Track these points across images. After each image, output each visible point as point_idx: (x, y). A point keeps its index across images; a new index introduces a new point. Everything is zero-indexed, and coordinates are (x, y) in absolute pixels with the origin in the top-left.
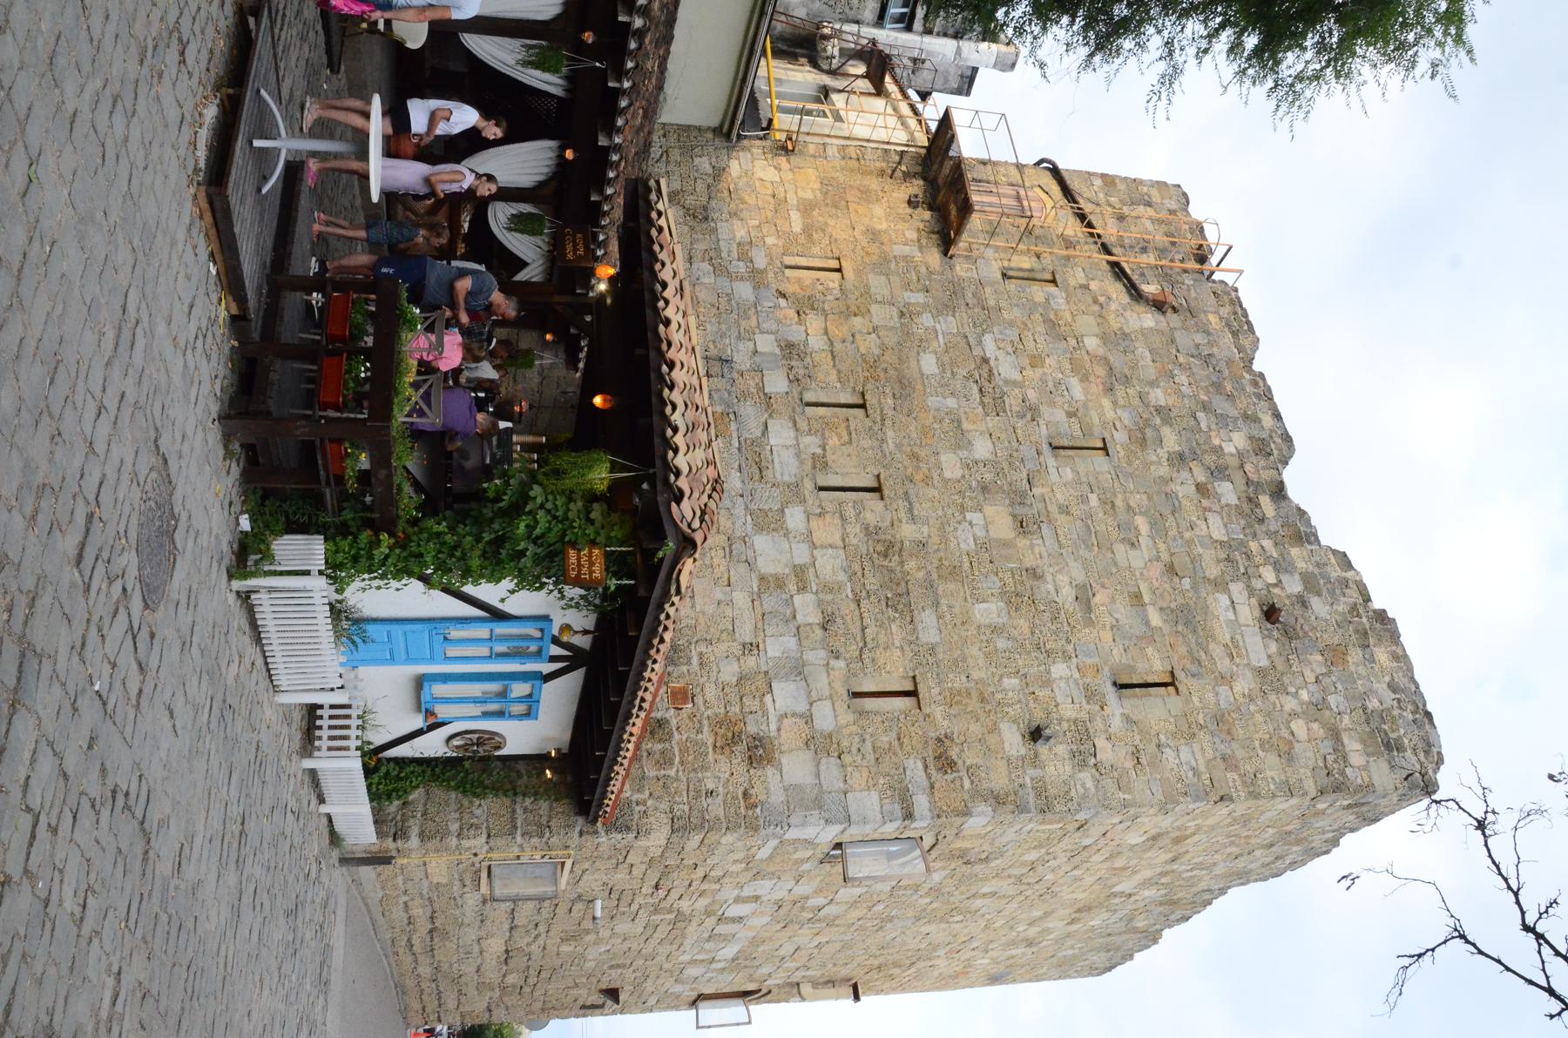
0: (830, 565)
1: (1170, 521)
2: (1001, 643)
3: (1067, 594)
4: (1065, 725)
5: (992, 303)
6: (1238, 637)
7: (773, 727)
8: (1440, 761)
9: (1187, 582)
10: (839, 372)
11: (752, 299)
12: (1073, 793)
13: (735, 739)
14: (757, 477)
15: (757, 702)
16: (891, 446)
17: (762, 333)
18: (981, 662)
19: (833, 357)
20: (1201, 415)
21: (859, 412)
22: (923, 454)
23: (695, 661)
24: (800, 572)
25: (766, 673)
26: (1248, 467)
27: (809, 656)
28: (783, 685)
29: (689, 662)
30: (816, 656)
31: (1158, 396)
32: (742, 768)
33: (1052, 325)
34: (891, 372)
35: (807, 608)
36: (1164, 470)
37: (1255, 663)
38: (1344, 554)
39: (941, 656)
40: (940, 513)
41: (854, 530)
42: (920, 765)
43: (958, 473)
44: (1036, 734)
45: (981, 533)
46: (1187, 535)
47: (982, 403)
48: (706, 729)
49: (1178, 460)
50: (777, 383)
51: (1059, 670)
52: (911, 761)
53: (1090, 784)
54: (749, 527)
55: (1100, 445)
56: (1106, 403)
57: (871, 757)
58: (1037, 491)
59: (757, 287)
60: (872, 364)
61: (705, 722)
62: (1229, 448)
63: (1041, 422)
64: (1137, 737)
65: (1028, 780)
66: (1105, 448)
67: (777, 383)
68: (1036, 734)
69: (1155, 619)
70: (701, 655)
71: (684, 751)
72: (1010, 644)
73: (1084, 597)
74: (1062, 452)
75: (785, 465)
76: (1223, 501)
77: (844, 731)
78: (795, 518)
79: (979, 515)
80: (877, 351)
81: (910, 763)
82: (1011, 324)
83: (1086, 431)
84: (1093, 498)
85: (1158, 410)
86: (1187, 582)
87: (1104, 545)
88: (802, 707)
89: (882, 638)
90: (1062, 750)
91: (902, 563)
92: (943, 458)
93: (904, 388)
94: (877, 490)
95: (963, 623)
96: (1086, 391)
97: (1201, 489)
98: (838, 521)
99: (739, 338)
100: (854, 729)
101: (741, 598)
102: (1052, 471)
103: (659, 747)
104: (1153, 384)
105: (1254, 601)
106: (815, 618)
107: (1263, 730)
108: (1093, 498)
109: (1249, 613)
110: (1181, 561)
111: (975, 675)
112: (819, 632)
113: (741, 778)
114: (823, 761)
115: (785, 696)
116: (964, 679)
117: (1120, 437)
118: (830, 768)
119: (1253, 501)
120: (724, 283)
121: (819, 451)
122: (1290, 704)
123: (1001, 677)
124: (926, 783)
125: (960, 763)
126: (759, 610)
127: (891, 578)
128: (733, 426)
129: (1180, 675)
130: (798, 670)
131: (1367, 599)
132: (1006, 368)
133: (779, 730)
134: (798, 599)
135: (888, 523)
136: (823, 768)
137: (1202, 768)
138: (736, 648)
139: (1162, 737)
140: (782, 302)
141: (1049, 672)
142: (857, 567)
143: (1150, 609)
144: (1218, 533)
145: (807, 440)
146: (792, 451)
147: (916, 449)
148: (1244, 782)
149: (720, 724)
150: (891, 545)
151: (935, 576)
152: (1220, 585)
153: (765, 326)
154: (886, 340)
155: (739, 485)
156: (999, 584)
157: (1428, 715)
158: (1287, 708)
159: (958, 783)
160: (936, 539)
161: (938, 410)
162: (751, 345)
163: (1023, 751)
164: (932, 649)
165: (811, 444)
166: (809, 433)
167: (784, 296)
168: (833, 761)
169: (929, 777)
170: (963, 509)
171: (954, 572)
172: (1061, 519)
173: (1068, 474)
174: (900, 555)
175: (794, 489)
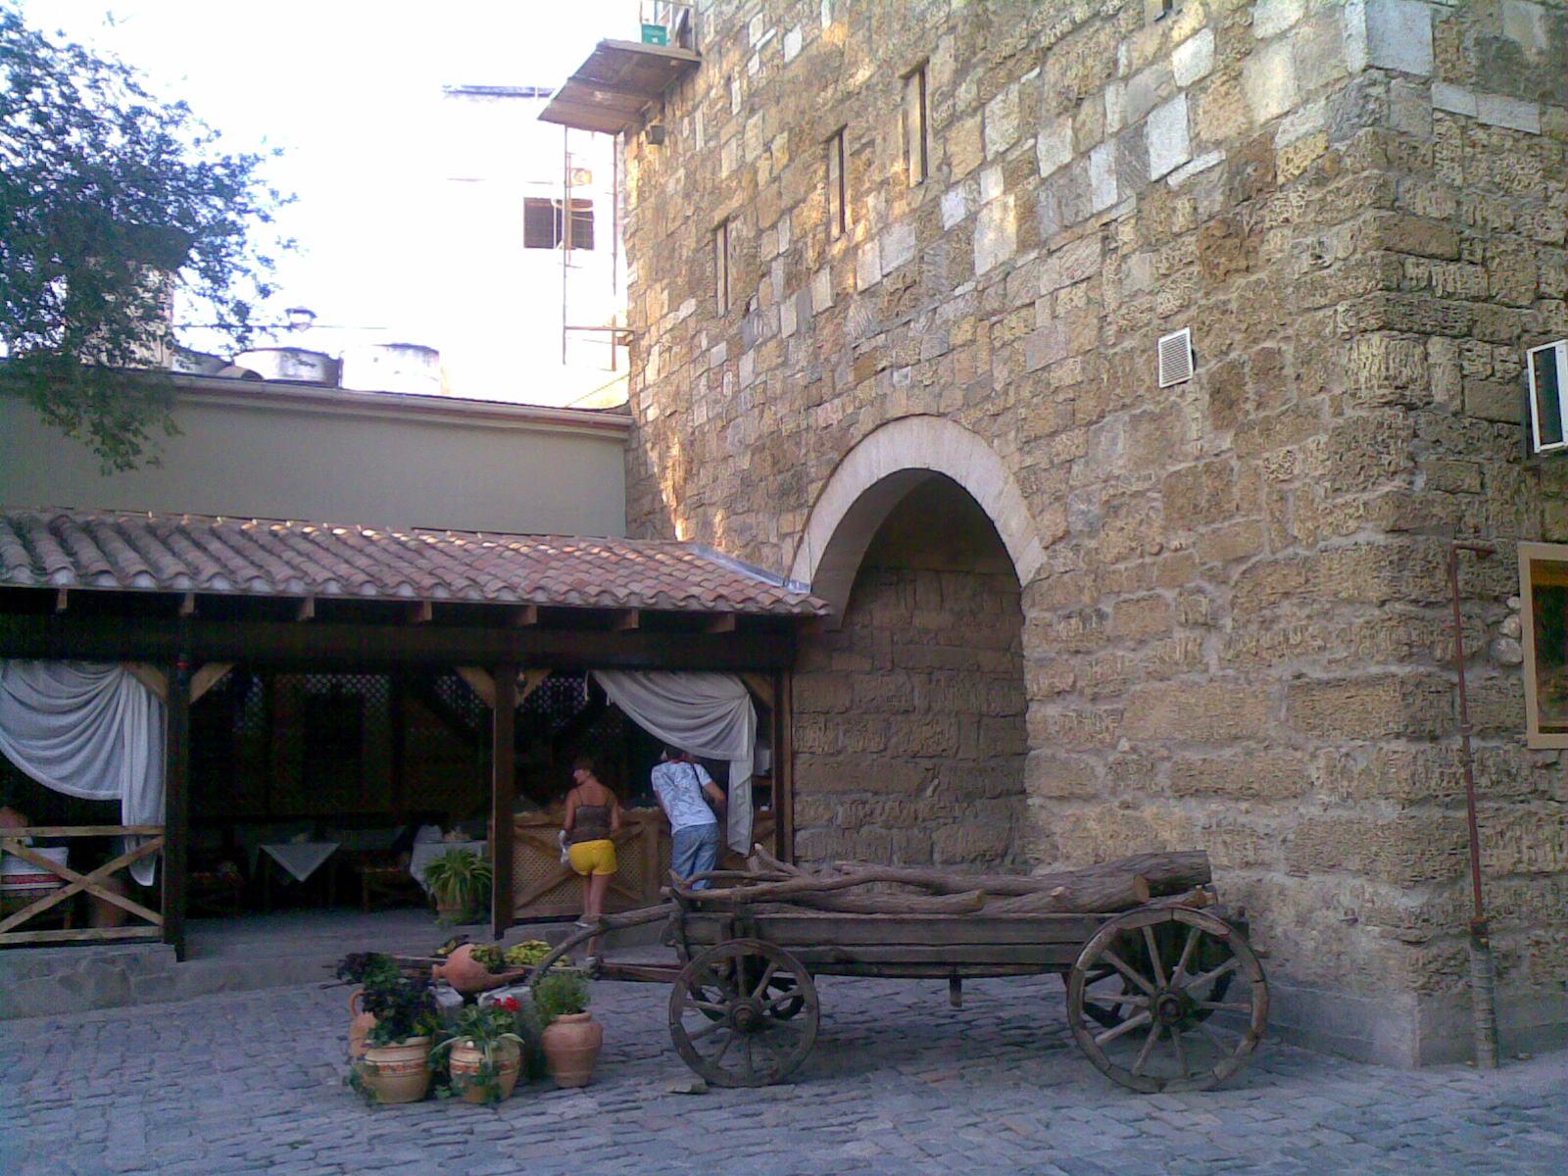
28: (1153, 159)
103: (1250, 388)
133: (1218, 144)
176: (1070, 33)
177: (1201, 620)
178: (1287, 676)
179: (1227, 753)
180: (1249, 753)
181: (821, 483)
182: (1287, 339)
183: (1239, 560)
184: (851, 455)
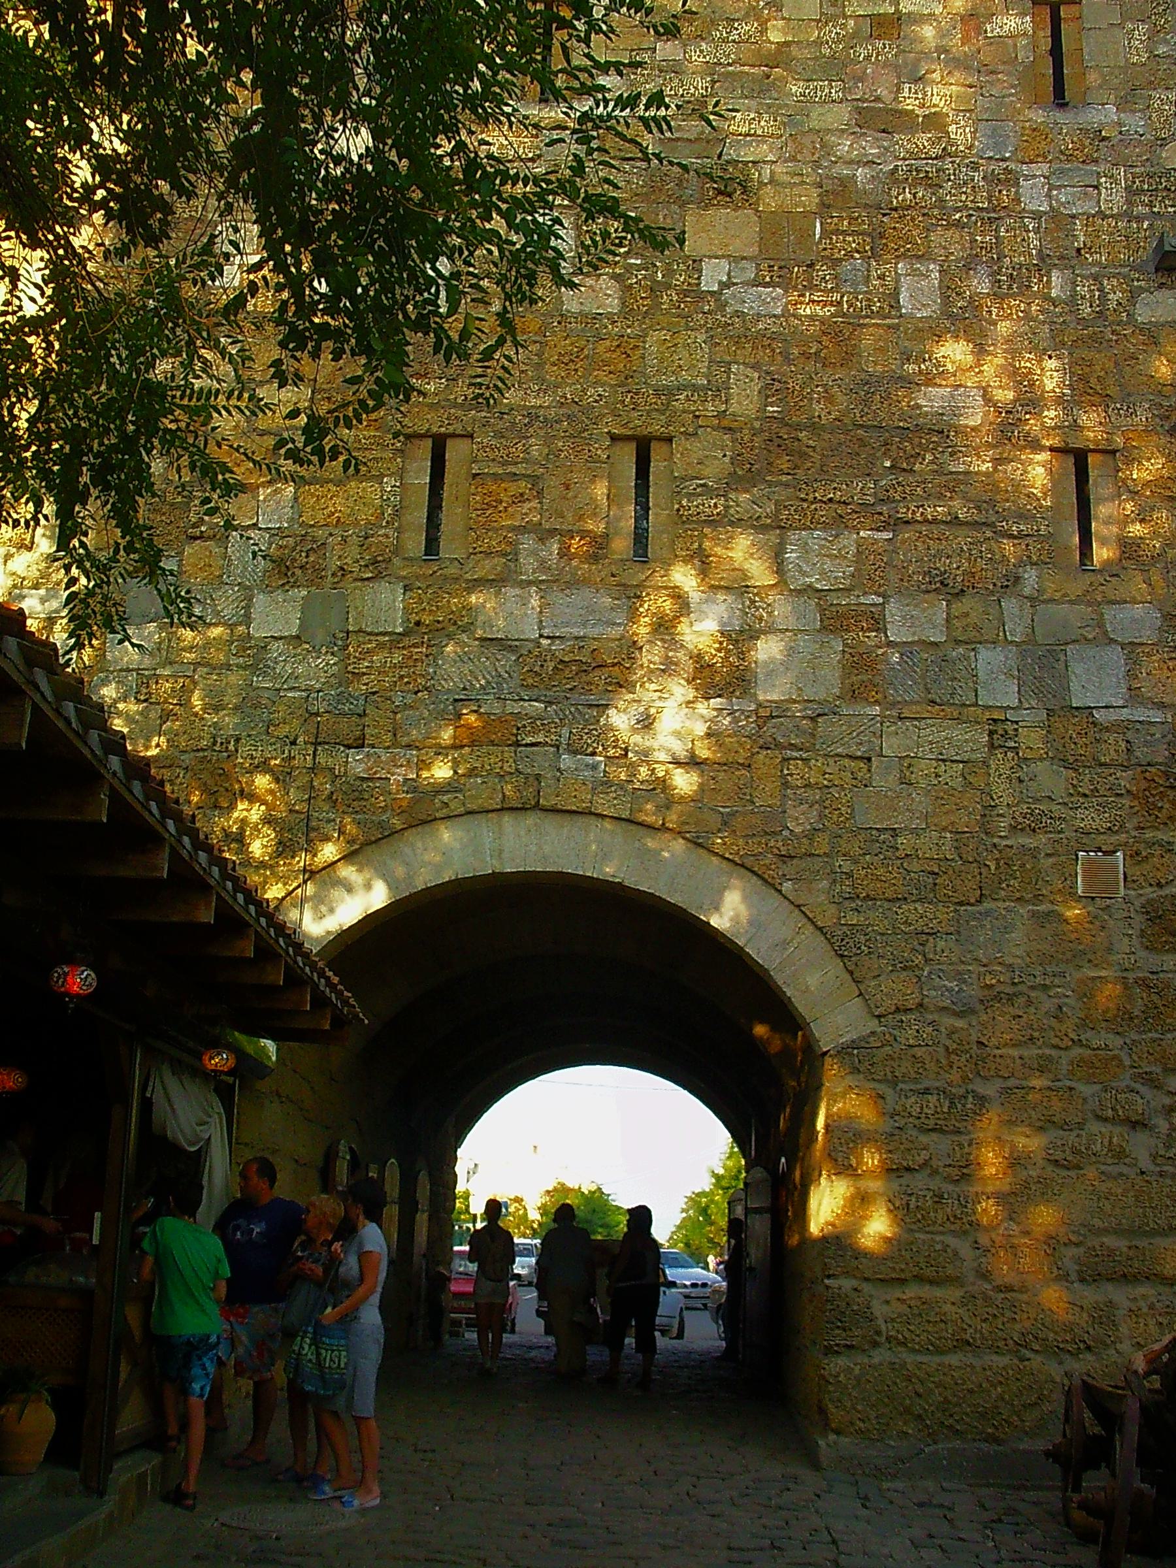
7: (1157, 716)
16: (547, 400)
17: (247, 620)
21: (455, 452)
24: (834, 621)
25: (1050, 712)
27: (1016, 630)
28: (1074, 686)
29: (1034, 853)
35: (909, 622)
48: (1160, 835)
50: (387, 605)
61: (1149, 835)
67: (387, 605)
88: (1115, 656)
91: (814, 427)
112: (965, 604)
115: (1095, 683)
133: (1162, 706)
138: (1001, 763)
141: (1037, 216)
145: (528, 565)
146: (558, 598)
149: (1151, 809)
150: (776, 444)
160: (763, 356)
170: (693, 293)
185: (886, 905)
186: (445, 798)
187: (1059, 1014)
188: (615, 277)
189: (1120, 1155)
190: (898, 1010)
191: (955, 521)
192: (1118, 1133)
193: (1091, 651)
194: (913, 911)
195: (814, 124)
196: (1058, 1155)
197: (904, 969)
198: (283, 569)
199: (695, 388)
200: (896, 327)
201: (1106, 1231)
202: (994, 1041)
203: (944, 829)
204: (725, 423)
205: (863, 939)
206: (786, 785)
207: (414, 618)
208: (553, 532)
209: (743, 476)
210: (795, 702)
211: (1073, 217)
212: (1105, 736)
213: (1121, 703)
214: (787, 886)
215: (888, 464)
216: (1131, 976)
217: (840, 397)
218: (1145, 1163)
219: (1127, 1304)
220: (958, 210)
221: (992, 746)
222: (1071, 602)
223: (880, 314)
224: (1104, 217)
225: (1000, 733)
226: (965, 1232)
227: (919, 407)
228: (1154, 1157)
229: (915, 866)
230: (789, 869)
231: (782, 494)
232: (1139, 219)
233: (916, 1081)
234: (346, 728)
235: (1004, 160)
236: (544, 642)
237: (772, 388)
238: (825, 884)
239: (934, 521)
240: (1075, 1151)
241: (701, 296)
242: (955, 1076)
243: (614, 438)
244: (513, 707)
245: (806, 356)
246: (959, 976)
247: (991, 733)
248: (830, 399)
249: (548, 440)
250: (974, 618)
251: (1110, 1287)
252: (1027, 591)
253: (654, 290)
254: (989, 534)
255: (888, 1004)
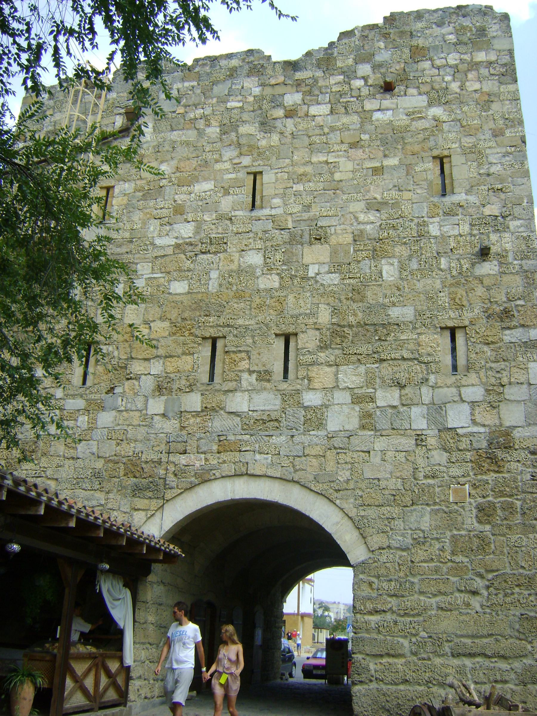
0: (351, 376)
1: (317, 139)
2: (414, 265)
3: (372, 216)
4: (475, 232)
5: (127, 235)
6: (406, 111)
7: (482, 430)
8: (491, 8)
9: (363, 137)
10: (184, 354)
11: (114, 413)
12: (525, 234)
13: (493, 459)
14: (276, 424)
15: (464, 439)
16: (252, 322)
18: (429, 282)
19: (171, 356)
20: (229, 105)
21: (220, 344)
22: (258, 301)
23: (431, 481)
24: (357, 400)
25: (439, 431)
26: (273, 82)
27: (426, 399)
28: (449, 419)
29: (433, 486)
30: (426, 394)
31: (213, 131)
32: (515, 454)
33: (147, 195)
34: (186, 315)
35: (387, 397)
36: (275, 138)
37: (425, 104)
38: (341, 34)
39: (425, 308)
40: (308, 294)
41: (322, 356)
42: (507, 332)
43: (276, 278)
44: (484, 253)
45: (326, 268)
46: (326, 130)
47: (215, 253)
48: (484, 477)
49: (266, 125)
50: (194, 401)
51: (434, 230)
52: (505, 337)
53: (518, 223)
54: (320, 433)
55: (252, 177)
56: (218, 166)
57: (502, 365)
58: (290, 225)
59: (103, 409)
60: (177, 329)
61: (479, 477)
62: (257, 91)
63: (233, 214)
64: (483, 187)
65: (515, 262)
66: (255, 174)
67: (194, 401)
68: (484, 253)
69: (393, 161)
70: (426, 477)
71: (502, 494)
72: (414, 260)
73: (374, 206)
74: (258, 203)
75: (267, 402)
76: (299, 102)
77: (484, 380)
78: (312, 399)
79: (311, 267)
80: (167, 324)
81: (507, 339)
82: (144, 223)
83: (238, 184)
84: (296, 187)
85: (224, 133)
86: (363, 137)
87: (336, 187)
88: (466, 408)
89: (411, 346)
90: (494, 237)
91: (350, 326)
92: (262, 286)
93: (202, 305)
94: (287, 338)
95: (399, 289)
96: (206, 179)
97: (290, 114)
98: (315, 368)
99: (150, 426)
100: (482, 373)
101: (380, 444)
102: (273, 212)
103: (499, 512)
104: (201, 133)
105: (378, 96)
106: (396, 392)
107: (470, 110)
108: (296, 187)
109: (387, 102)
110: (348, 137)
111: (438, 284)
112: (407, 390)
113: (523, 455)
114: (507, 397)
115: (458, 418)
116: (442, 294)
117: (246, 161)
118: (511, 392)
119: (298, 84)
120: (98, 434)
121: (254, 376)
122: (455, 86)
123: (441, 270)
124: (521, 330)
125: (505, 305)
126: (390, 432)
127: (360, 334)
128: (231, 438)
129: (436, 153)
130: (437, 409)
131: (374, 27)
132: (186, 231)
133: (484, 426)
134: (380, 403)
135: (317, 333)
136: (512, 398)
137: (504, 150)
138: (420, 451)
139: (481, 171)
140: (117, 390)
141: (436, 237)
142: (354, 358)
143: (386, 163)
144: (325, 109)
145: (244, 384)
147: (254, 305)
148: (512, 126)
149: (480, 466)
150: (334, 334)
151: (360, 304)
152: (366, 116)
153: (140, 406)
154: (157, 316)
155: (283, 438)
156: (367, 261)
157: (459, 7)
158: (458, 90)
159: (520, 308)
161: (220, 285)
162: (156, 418)
163: (496, 263)
164: (419, 314)
165: (248, 380)
166: (239, 380)
167: (113, 389)
168: (507, 390)
169: (515, 327)
171: (357, 293)
172: (315, 211)
173: (277, 201)
174: (344, 326)
175: (284, 396)
176: (399, 359)
177: (473, 590)
178: (518, 613)
179: (485, 640)
180: (497, 640)
181: (179, 491)
182: (517, 499)
183: (493, 571)
184: (208, 483)
185: (375, 508)
186: (214, 472)
187: (442, 549)
188: (278, 274)
189: (468, 605)
190: (380, 549)
191: (403, 359)
192: (466, 597)
193: (455, 406)
194: (385, 510)
195: (351, 210)
196: (443, 605)
197: (382, 532)
198: (160, 389)
199: (306, 314)
200: (381, 285)
201: (462, 636)
202: (417, 560)
203: (398, 478)
204: (317, 327)
205: (366, 521)
206: (338, 463)
207: (204, 405)
208: (254, 371)
209: (323, 347)
210: (341, 431)
211: (450, 237)
212: (461, 439)
213: (467, 425)
214: (338, 502)
215: (377, 338)
216: (472, 533)
217: (360, 314)
218: (478, 609)
219: (471, 665)
220: (405, 238)
221: (417, 445)
222: (448, 387)
223: (375, 280)
224: (461, 236)
225: (420, 439)
226: (406, 636)
227: (389, 315)
228: (482, 606)
229: (387, 492)
230: (339, 495)
231: (337, 352)
232: (475, 236)
233: (386, 576)
234: (180, 447)
235: (423, 217)
236: (250, 413)
237: (335, 311)
238: (352, 500)
239: (395, 359)
240: (450, 604)
241: (309, 279)
242: (402, 574)
243: (277, 335)
244: (240, 437)
245: (347, 299)
246: (403, 535)
247: (416, 440)
248: (355, 315)
249: (253, 337)
250: (410, 396)
251: (464, 659)
252: (431, 384)
253: (292, 277)
254: (416, 362)
255: (376, 546)
